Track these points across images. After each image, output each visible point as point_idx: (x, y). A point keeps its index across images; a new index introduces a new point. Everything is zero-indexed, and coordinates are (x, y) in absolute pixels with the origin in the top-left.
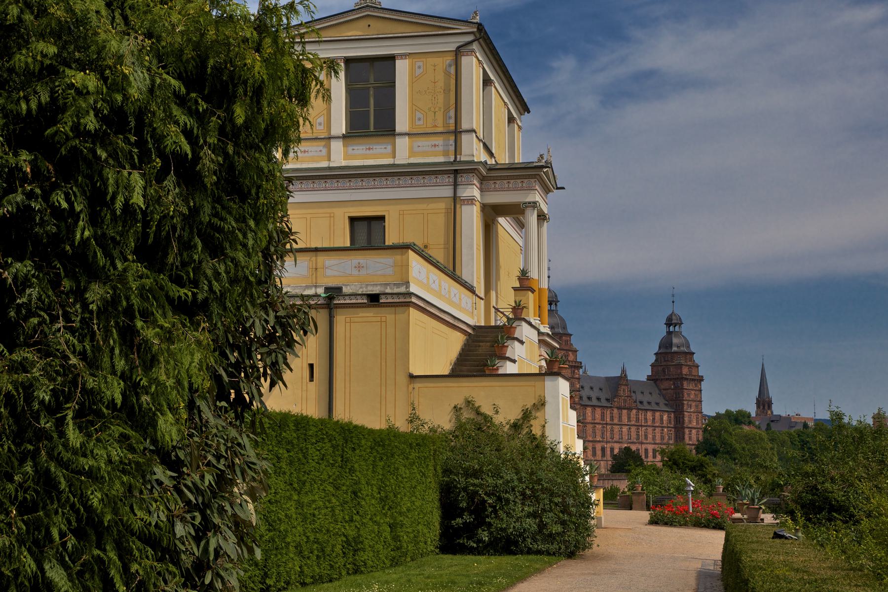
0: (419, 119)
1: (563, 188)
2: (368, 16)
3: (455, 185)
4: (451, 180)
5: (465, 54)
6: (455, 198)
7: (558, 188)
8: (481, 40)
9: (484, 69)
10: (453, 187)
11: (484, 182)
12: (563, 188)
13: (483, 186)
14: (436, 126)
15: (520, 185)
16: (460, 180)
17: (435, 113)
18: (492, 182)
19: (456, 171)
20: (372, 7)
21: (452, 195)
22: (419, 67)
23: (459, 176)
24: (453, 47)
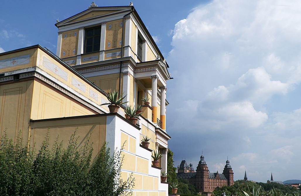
0: (109, 45)
1: (173, 78)
2: (93, 11)
3: (121, 68)
4: (119, 66)
5: (127, 18)
6: (120, 72)
7: (170, 78)
9: (138, 30)
10: (120, 69)
12: (173, 78)
15: (150, 70)
17: (115, 42)
18: (139, 69)
19: (121, 62)
20: (94, 7)
21: (120, 72)
22: (110, 26)
23: (123, 64)
24: (122, 17)
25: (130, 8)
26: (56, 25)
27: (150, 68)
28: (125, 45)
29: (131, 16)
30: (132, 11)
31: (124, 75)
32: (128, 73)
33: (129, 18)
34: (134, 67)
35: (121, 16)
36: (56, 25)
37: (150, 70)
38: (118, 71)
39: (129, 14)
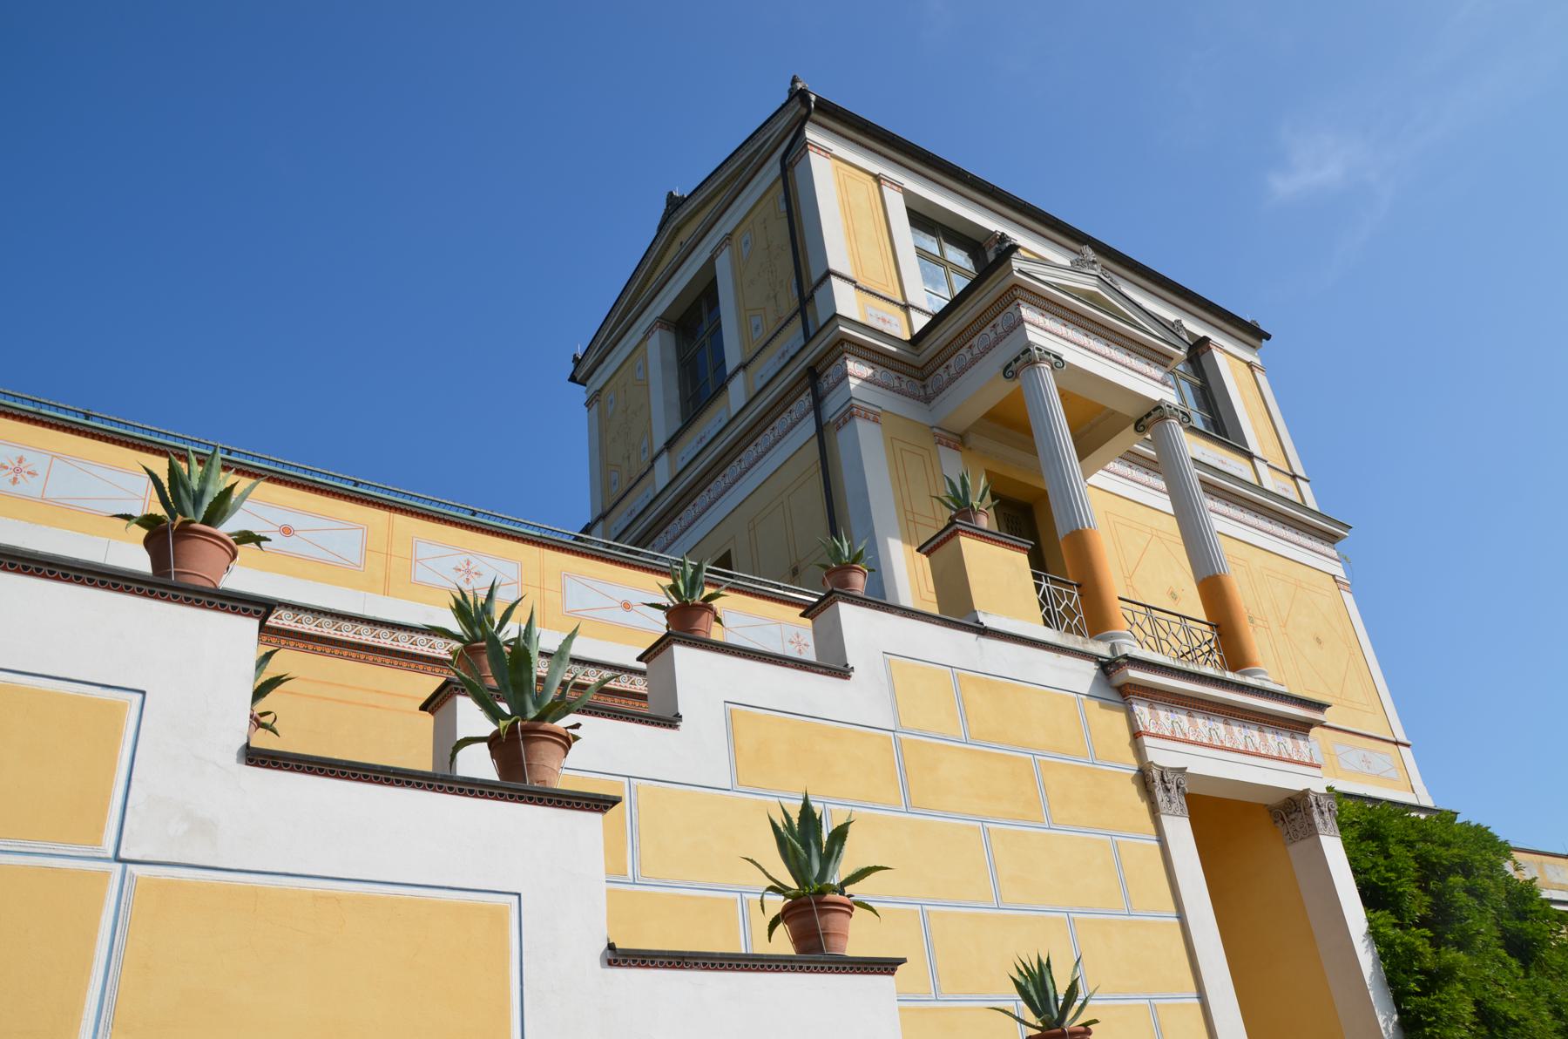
8: (814, 116)
10: (812, 414)
11: (929, 381)
13: (929, 391)
14: (780, 318)
16: (826, 386)
23: (822, 380)
25: (794, 107)
26: (573, 379)
27: (987, 330)
28: (815, 276)
29: (811, 134)
30: (804, 111)
31: (839, 428)
32: (852, 406)
33: (802, 153)
34: (913, 371)
35: (772, 169)
36: (573, 379)
37: (992, 336)
38: (808, 427)
39: (800, 132)
